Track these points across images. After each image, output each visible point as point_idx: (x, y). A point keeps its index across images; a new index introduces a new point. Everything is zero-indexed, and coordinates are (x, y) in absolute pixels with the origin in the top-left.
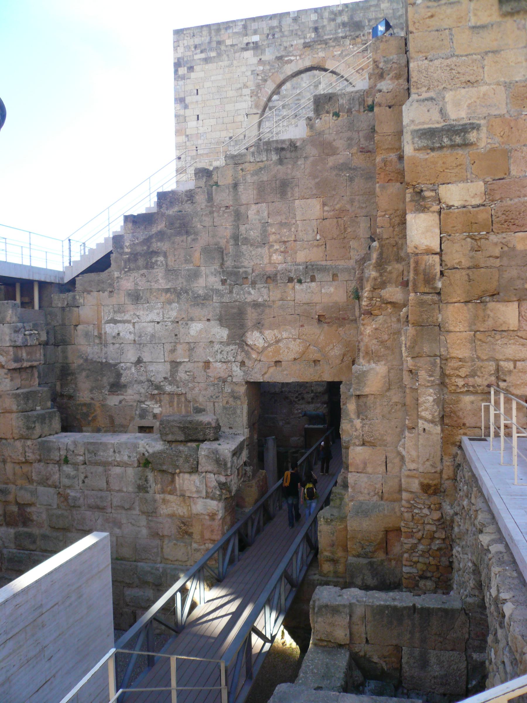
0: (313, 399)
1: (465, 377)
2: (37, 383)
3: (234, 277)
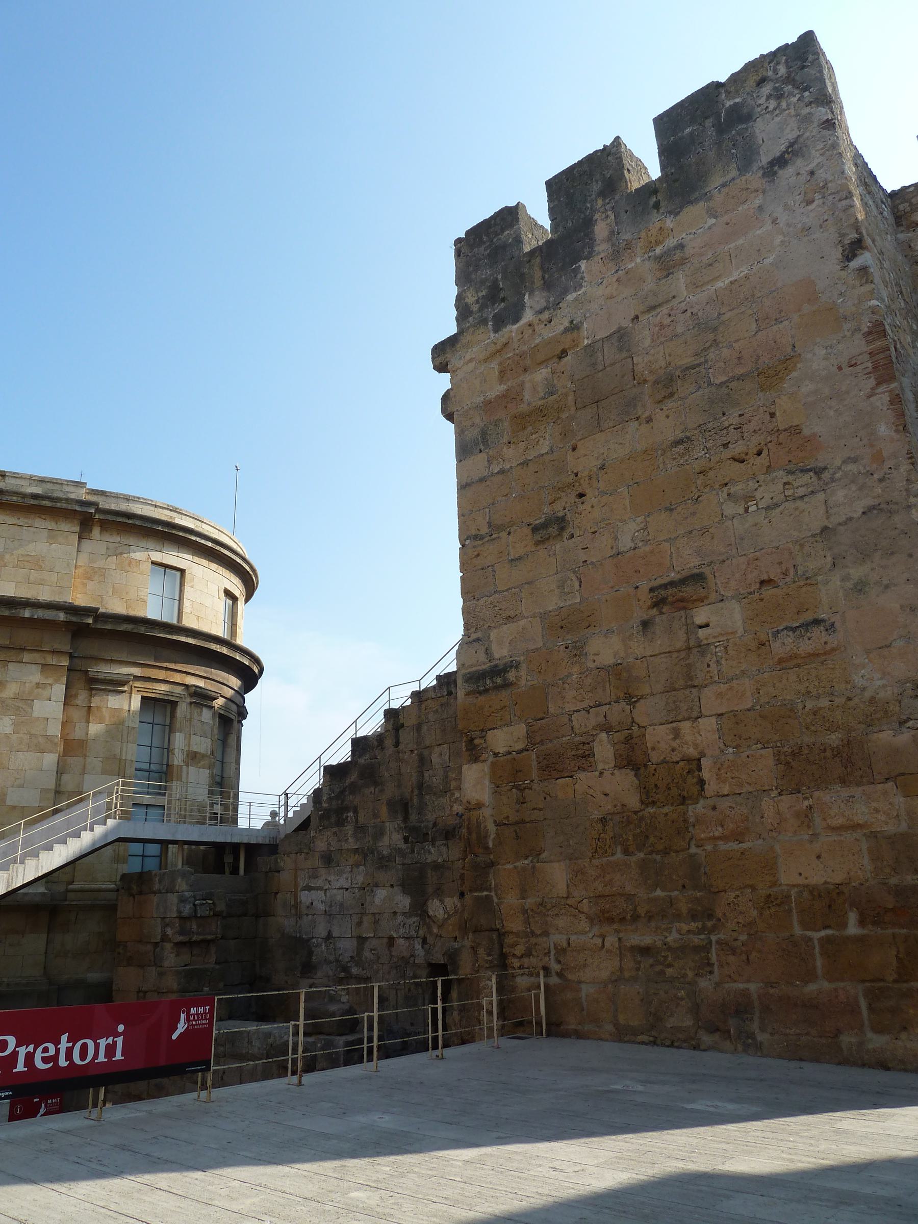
1: (522, 957)
2: (213, 959)
3: (417, 835)
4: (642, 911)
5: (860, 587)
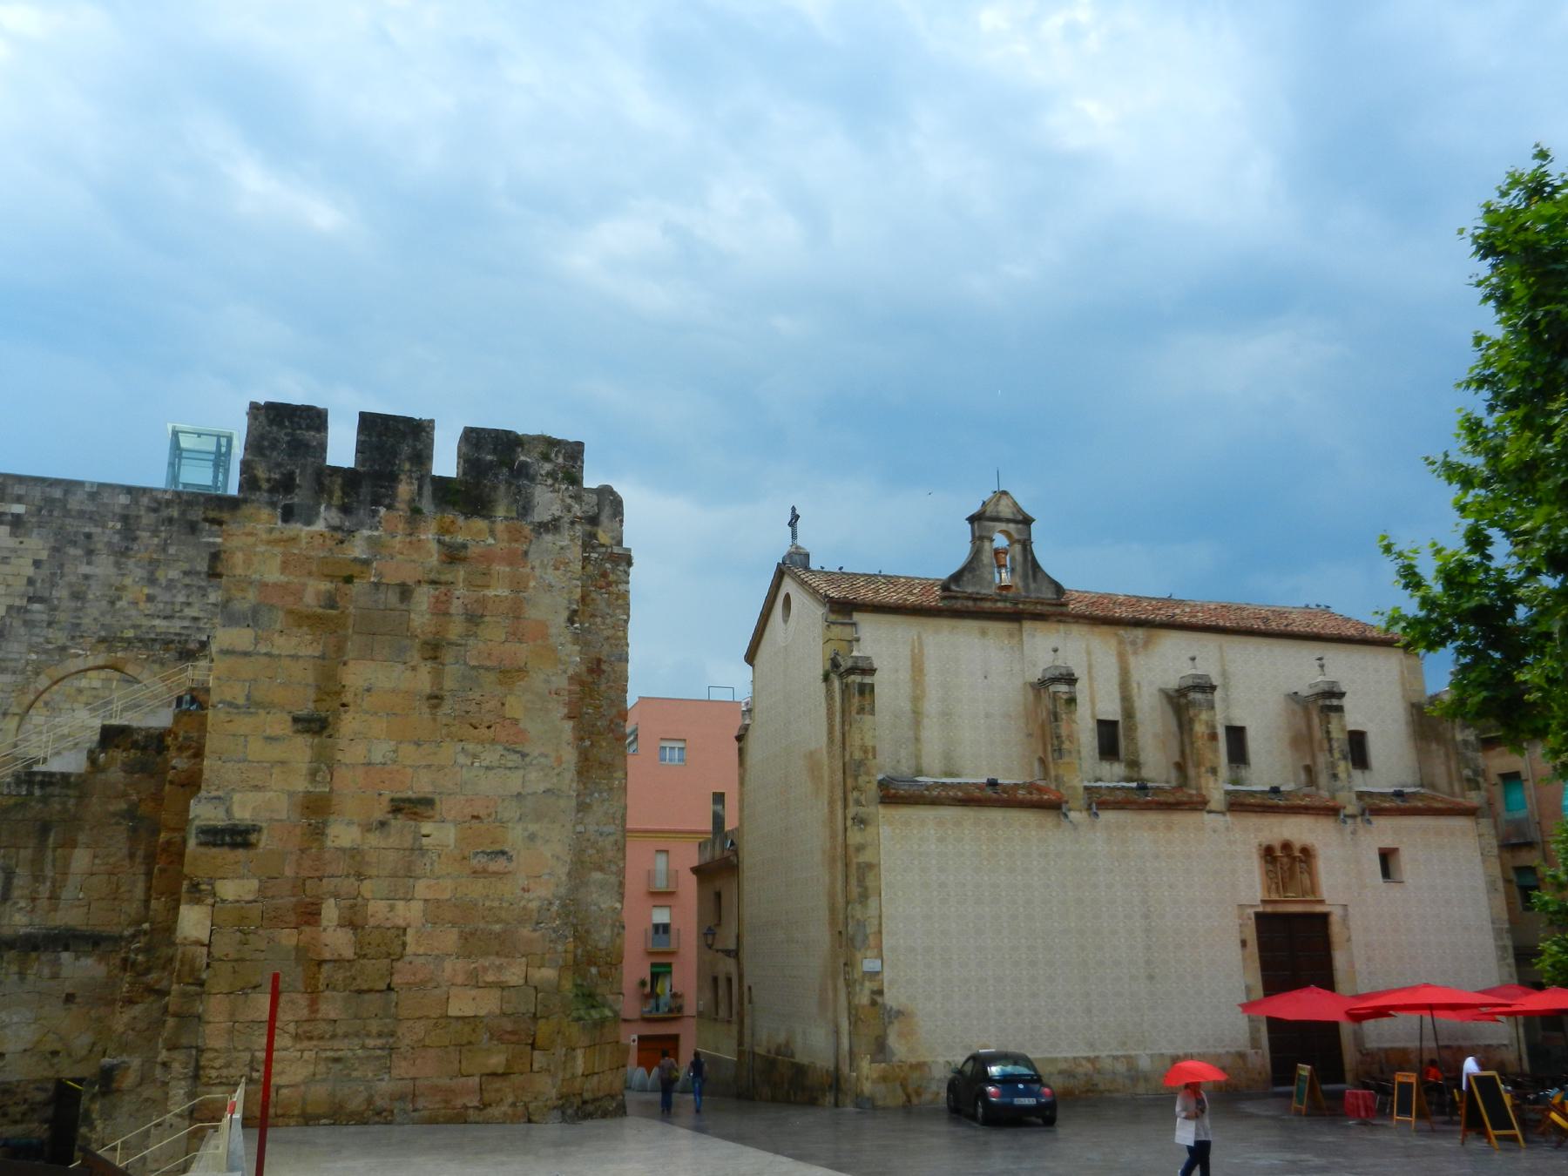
0: (24, 1114)
4: (340, 1031)
5: (532, 837)
